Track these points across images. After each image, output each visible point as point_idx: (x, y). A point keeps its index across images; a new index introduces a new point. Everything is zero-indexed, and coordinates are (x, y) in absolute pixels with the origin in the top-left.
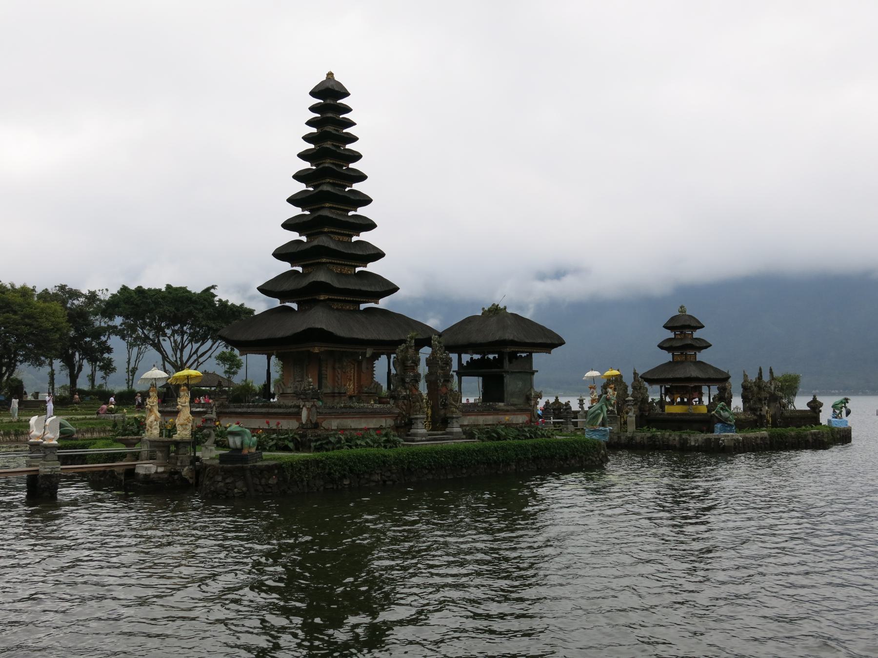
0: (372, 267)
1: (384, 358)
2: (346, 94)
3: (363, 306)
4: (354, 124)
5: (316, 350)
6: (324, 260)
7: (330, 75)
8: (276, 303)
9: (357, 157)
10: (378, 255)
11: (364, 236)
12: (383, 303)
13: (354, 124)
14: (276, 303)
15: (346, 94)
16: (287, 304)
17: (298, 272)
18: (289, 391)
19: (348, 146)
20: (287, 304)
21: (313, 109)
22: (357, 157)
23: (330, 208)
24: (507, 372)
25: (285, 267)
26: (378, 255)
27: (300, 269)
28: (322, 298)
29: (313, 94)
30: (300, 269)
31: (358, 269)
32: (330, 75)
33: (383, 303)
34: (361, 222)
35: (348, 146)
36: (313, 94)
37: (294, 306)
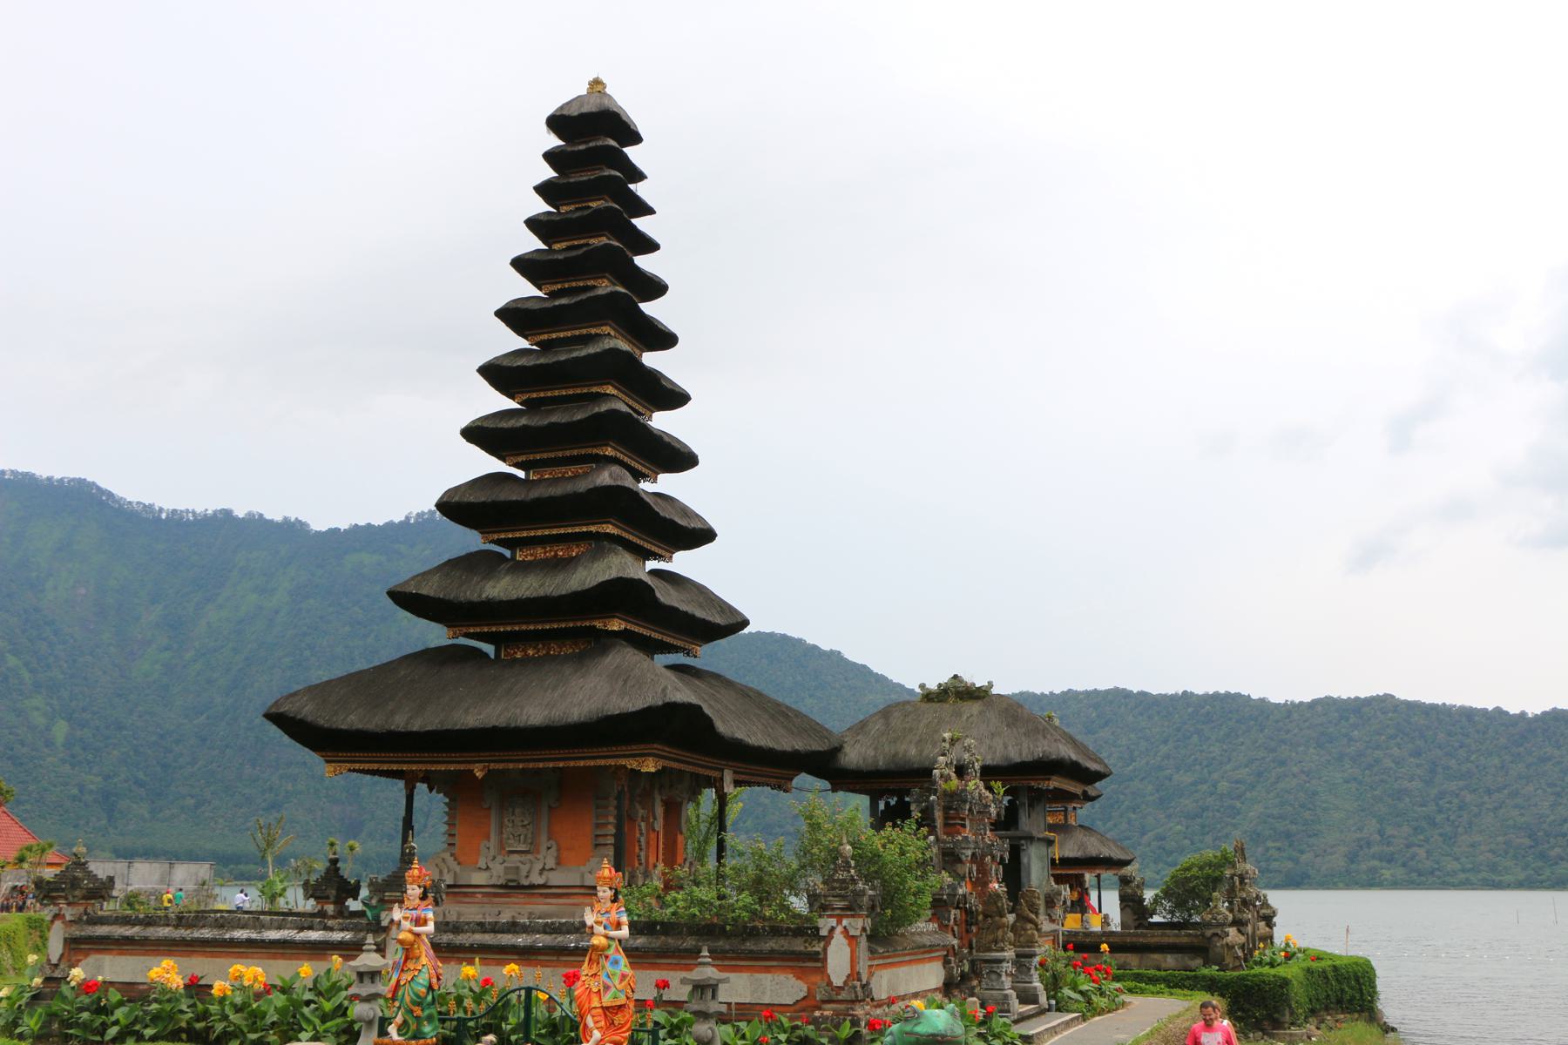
0: (684, 563)
1: (709, 795)
2: (635, 138)
4: (650, 211)
5: (650, 766)
6: (610, 529)
7: (596, 83)
8: (435, 635)
9: (655, 288)
10: (701, 536)
13: (650, 211)
15: (635, 138)
18: (478, 878)
20: (462, 641)
22: (655, 288)
24: (1031, 839)
25: (470, 540)
26: (701, 536)
28: (616, 625)
29: (557, 123)
32: (596, 83)
36: (557, 123)
37: (489, 649)
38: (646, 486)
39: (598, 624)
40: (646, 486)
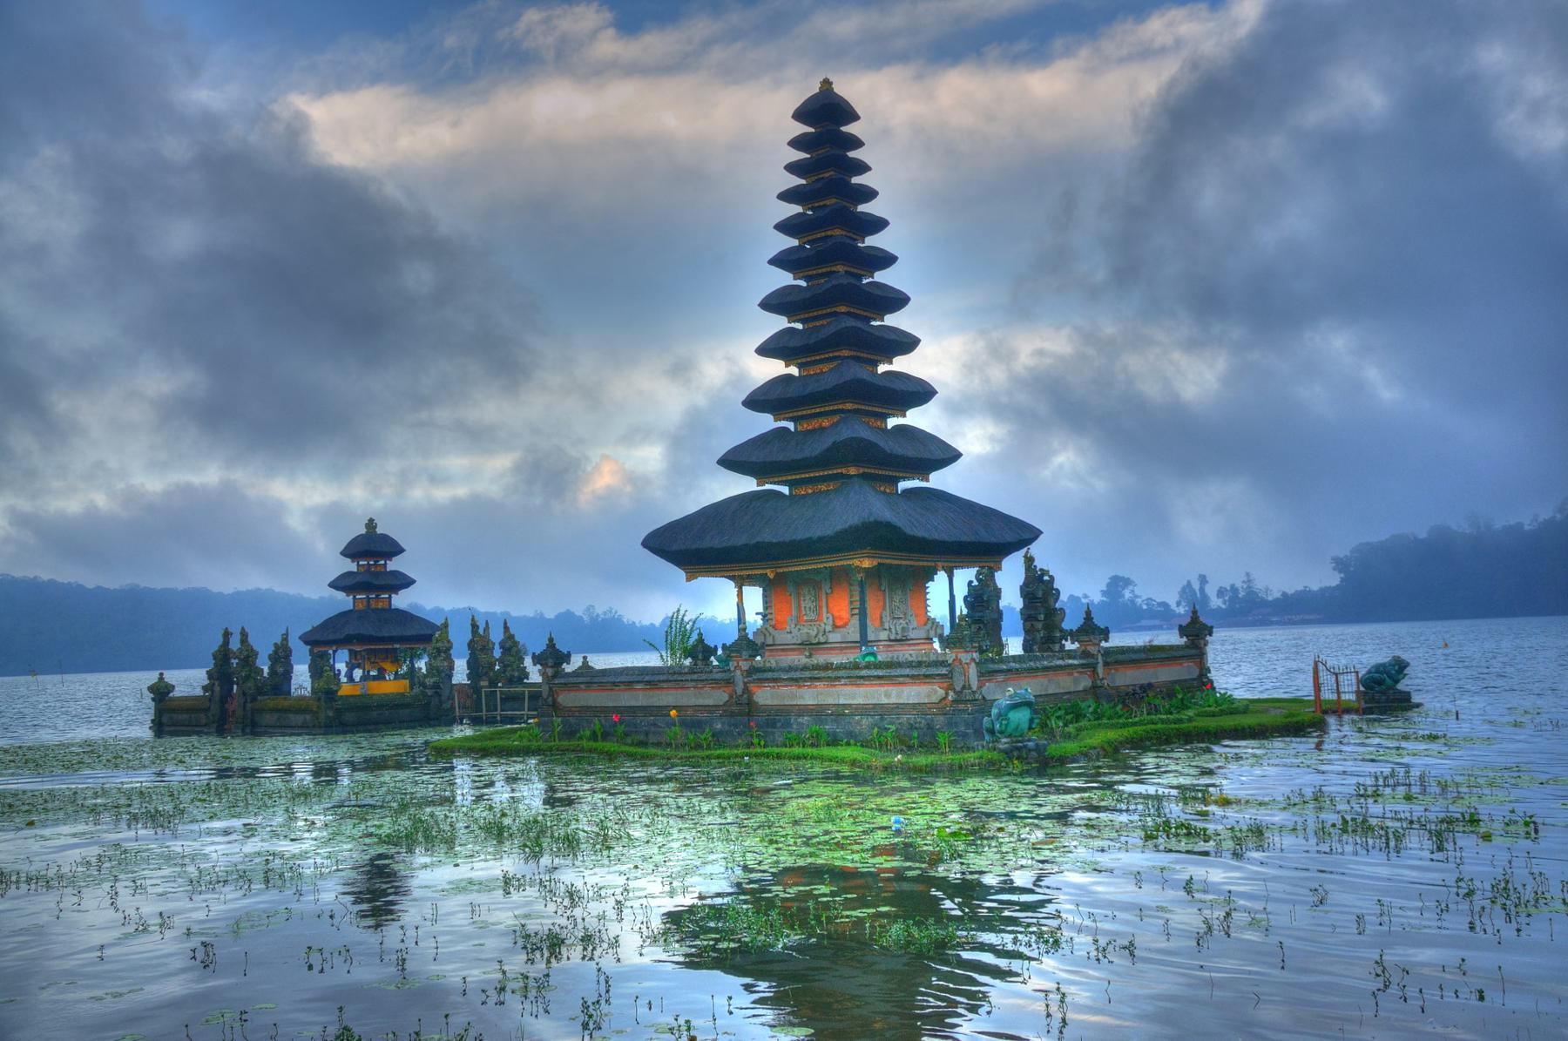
1: (941, 576)
2: (854, 117)
3: (903, 485)
11: (901, 364)
12: (939, 480)
14: (745, 485)
15: (854, 117)
16: (768, 487)
17: (785, 429)
19: (862, 208)
20: (768, 487)
21: (796, 143)
23: (849, 314)
25: (766, 422)
27: (791, 426)
30: (791, 426)
31: (892, 422)
33: (939, 480)
34: (893, 337)
35: (862, 208)
36: (800, 115)
38: (882, 368)
39: (844, 471)
40: (882, 368)
